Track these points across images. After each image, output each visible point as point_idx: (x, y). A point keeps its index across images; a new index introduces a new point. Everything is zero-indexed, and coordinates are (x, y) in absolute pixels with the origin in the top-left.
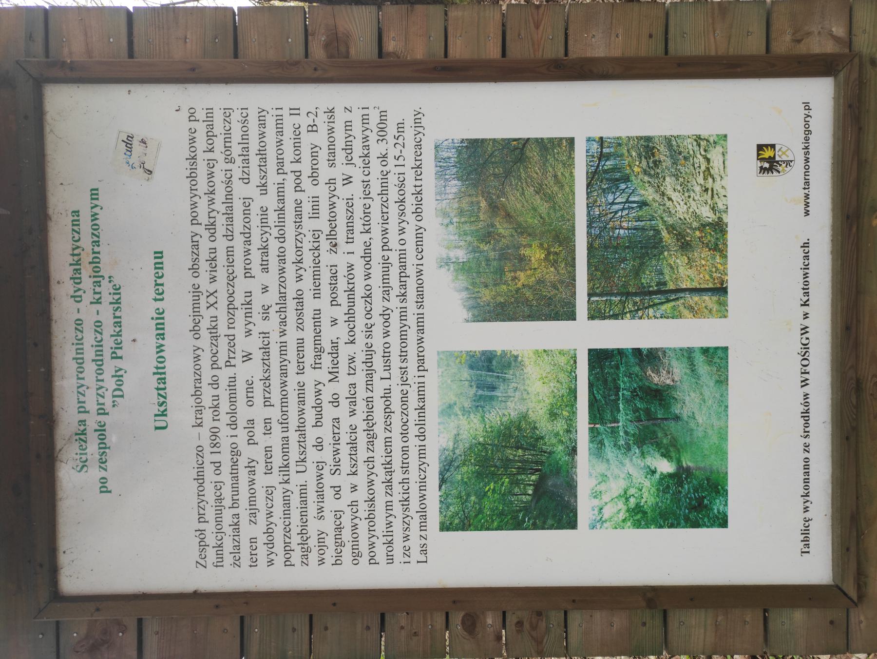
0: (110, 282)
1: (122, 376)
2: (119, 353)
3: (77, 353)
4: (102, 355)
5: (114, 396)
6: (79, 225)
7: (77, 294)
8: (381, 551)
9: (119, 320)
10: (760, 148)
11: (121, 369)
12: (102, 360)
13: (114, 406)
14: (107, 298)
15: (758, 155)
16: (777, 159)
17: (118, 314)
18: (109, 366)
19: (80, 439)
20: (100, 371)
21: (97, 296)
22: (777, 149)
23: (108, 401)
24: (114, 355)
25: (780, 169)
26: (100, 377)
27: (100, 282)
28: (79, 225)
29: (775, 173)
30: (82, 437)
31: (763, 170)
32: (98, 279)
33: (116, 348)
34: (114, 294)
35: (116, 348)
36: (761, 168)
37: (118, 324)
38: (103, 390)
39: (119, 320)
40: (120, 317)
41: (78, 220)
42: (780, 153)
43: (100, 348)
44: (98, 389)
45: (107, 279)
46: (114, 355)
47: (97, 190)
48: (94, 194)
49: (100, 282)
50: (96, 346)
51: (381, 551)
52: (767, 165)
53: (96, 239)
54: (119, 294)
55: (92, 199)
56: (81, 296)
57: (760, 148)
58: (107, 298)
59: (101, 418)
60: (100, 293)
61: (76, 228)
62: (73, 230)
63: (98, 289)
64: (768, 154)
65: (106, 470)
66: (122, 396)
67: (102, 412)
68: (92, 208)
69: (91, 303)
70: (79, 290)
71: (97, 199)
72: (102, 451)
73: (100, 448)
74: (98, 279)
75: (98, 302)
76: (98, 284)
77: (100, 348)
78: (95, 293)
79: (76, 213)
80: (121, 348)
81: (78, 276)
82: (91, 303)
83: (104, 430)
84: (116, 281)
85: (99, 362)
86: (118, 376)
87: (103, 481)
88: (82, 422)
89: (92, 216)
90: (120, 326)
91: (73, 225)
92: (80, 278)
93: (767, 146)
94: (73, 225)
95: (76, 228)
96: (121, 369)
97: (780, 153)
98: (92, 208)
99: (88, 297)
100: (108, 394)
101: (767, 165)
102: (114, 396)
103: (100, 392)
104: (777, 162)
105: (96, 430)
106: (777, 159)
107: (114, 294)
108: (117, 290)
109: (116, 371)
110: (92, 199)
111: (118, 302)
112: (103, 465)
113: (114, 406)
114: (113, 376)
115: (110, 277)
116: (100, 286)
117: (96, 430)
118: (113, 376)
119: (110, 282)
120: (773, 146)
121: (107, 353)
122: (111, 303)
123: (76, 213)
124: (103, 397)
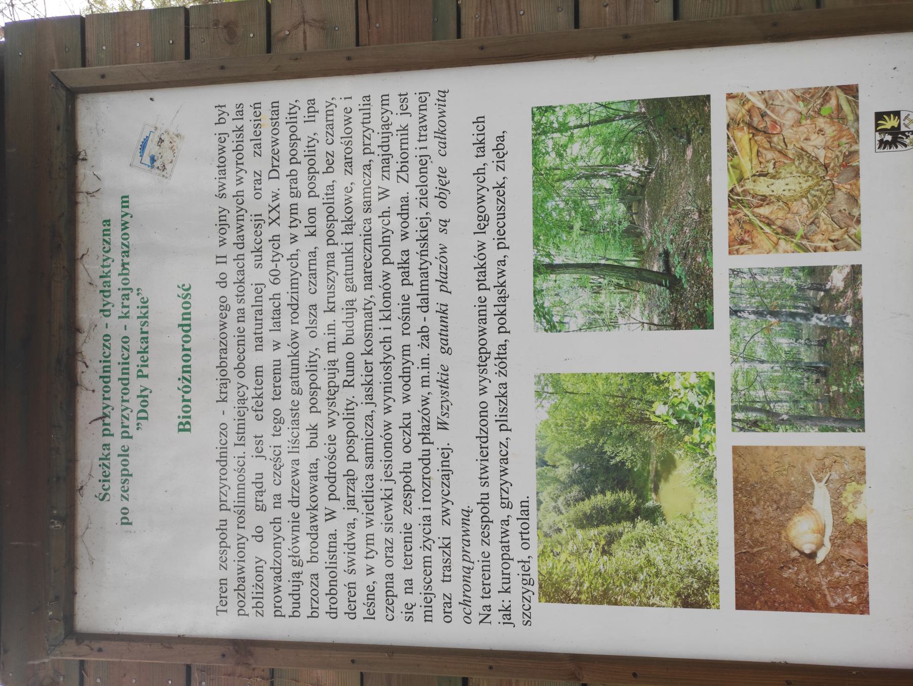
0: (138, 294)
1: (147, 396)
2: (145, 371)
3: (104, 372)
4: (128, 374)
5: (139, 418)
6: (109, 235)
7: (106, 308)
8: (324, 603)
9: (145, 335)
10: (879, 116)
11: (146, 389)
12: (128, 379)
13: (138, 429)
14: (134, 312)
15: (877, 125)
16: (903, 129)
17: (145, 329)
18: (135, 385)
19: (104, 464)
20: (125, 390)
21: (125, 310)
22: (903, 115)
23: (132, 422)
24: (140, 374)
25: (907, 141)
26: (126, 397)
27: (128, 295)
28: (109, 235)
29: (900, 147)
30: (106, 462)
31: (883, 144)
32: (126, 292)
33: (142, 366)
34: (142, 307)
35: (142, 366)
36: (881, 141)
37: (145, 340)
38: (128, 411)
39: (145, 335)
40: (147, 333)
41: (109, 230)
42: (907, 122)
43: (126, 366)
44: (123, 411)
45: (135, 292)
46: (140, 374)
47: (127, 197)
48: (125, 201)
49: (128, 295)
50: (123, 363)
51: (324, 603)
52: (888, 138)
53: (126, 249)
54: (147, 307)
55: (123, 207)
56: (109, 311)
57: (879, 116)
58: (134, 312)
59: (126, 442)
60: (128, 307)
61: (106, 238)
62: (104, 240)
63: (126, 303)
64: (890, 123)
65: (127, 499)
66: (146, 418)
67: (127, 436)
68: (123, 216)
69: (120, 317)
70: (109, 303)
71: (128, 207)
72: (124, 478)
73: (123, 475)
74: (126, 292)
75: (126, 316)
76: (126, 297)
77: (126, 366)
78: (124, 307)
79: (107, 222)
80: (147, 366)
81: (107, 288)
82: (120, 317)
83: (128, 455)
84: (144, 294)
85: (125, 381)
86: (144, 398)
87: (125, 511)
88: (106, 446)
89: (123, 225)
90: (147, 342)
91: (104, 235)
92: (109, 291)
93: (888, 114)
94: (104, 235)
95: (106, 238)
96: (146, 389)
97: (907, 122)
98: (123, 216)
99: (117, 311)
100: (133, 417)
101: (888, 138)
102: (139, 418)
103: (125, 413)
104: (903, 133)
105: (119, 455)
106: (903, 129)
107: (142, 307)
108: (145, 303)
109: (142, 391)
110: (123, 207)
111: (145, 316)
112: (125, 494)
113: (138, 429)
114: (138, 396)
115: (138, 290)
116: (128, 299)
117: (119, 455)
118: (138, 396)
119: (138, 294)
120: (897, 114)
121: (133, 370)
122: (138, 317)
123: (107, 222)
124: (128, 419)
